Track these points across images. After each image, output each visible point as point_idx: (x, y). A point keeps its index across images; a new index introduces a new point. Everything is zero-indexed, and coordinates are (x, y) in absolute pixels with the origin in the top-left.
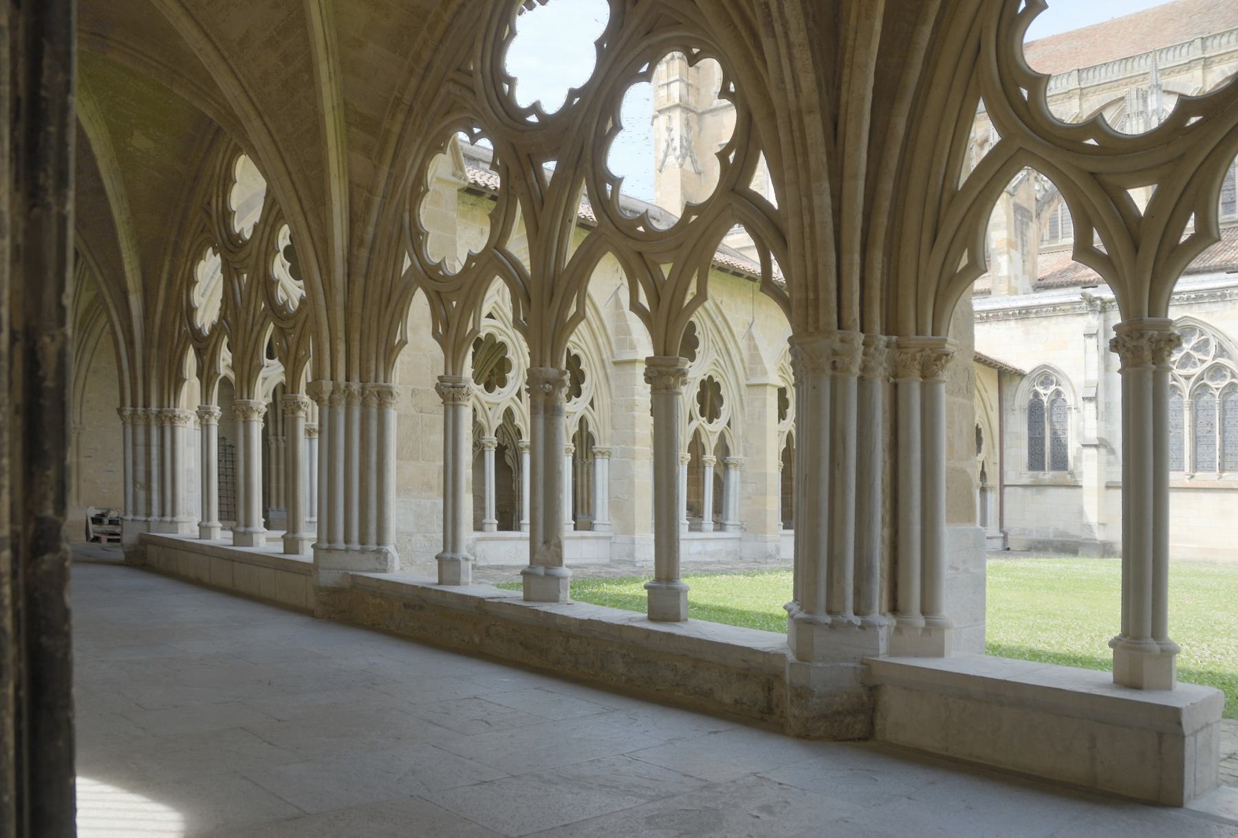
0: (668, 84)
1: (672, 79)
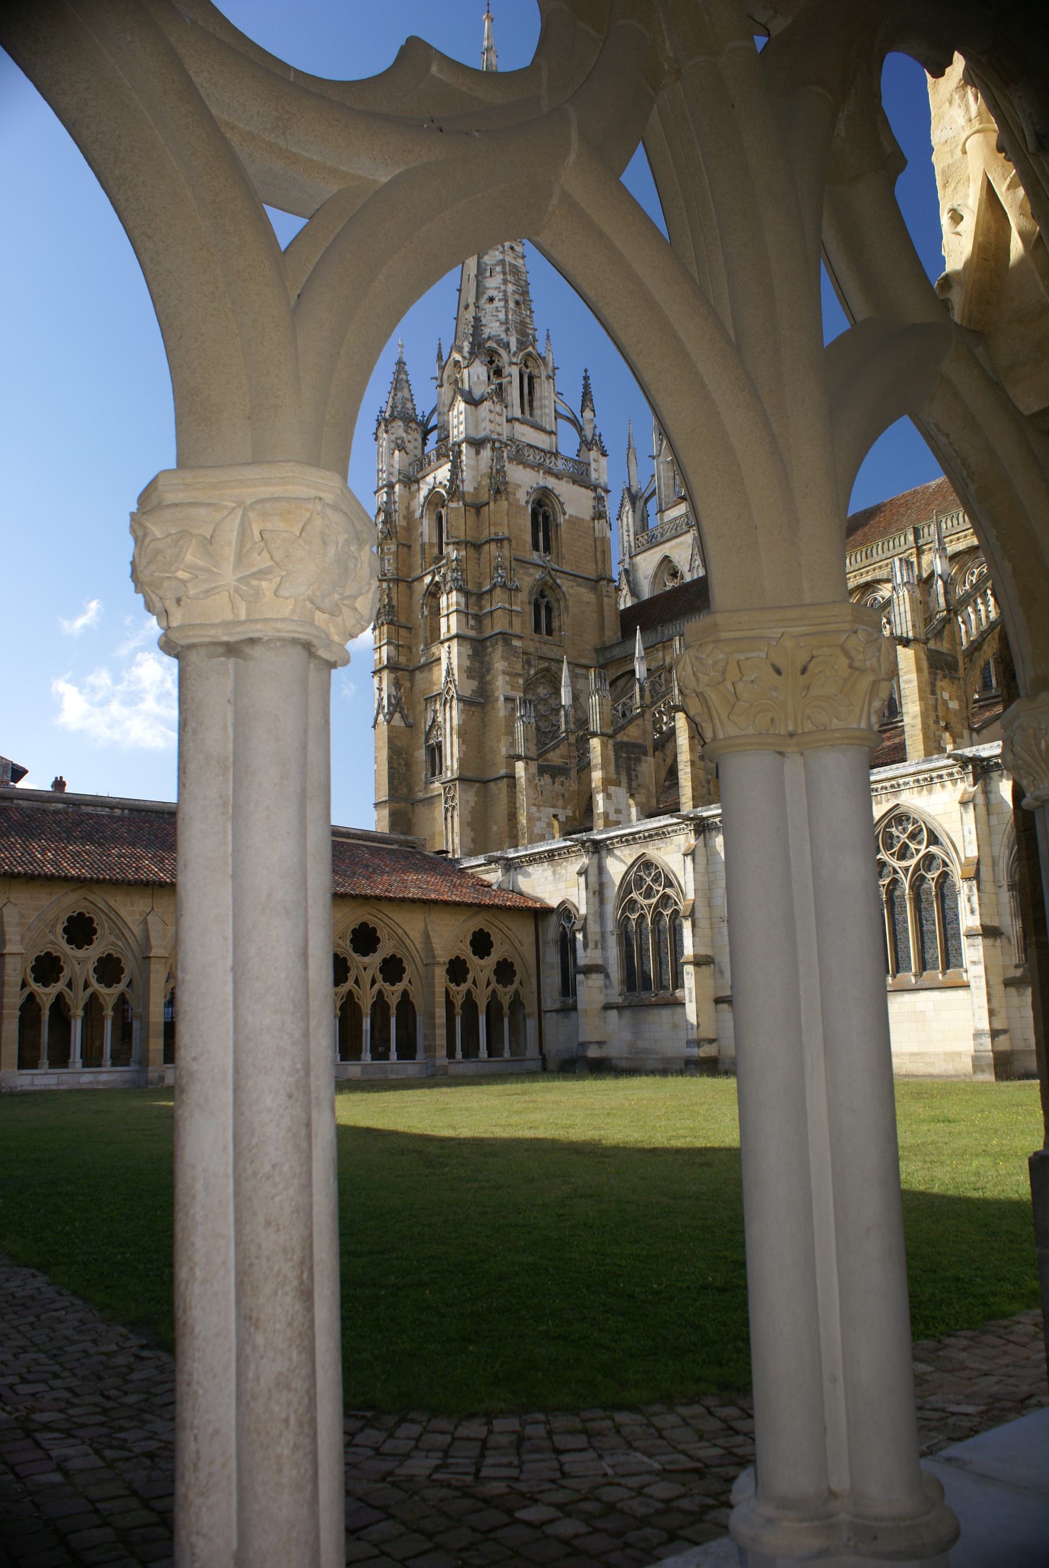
0: (380, 647)
1: (382, 643)
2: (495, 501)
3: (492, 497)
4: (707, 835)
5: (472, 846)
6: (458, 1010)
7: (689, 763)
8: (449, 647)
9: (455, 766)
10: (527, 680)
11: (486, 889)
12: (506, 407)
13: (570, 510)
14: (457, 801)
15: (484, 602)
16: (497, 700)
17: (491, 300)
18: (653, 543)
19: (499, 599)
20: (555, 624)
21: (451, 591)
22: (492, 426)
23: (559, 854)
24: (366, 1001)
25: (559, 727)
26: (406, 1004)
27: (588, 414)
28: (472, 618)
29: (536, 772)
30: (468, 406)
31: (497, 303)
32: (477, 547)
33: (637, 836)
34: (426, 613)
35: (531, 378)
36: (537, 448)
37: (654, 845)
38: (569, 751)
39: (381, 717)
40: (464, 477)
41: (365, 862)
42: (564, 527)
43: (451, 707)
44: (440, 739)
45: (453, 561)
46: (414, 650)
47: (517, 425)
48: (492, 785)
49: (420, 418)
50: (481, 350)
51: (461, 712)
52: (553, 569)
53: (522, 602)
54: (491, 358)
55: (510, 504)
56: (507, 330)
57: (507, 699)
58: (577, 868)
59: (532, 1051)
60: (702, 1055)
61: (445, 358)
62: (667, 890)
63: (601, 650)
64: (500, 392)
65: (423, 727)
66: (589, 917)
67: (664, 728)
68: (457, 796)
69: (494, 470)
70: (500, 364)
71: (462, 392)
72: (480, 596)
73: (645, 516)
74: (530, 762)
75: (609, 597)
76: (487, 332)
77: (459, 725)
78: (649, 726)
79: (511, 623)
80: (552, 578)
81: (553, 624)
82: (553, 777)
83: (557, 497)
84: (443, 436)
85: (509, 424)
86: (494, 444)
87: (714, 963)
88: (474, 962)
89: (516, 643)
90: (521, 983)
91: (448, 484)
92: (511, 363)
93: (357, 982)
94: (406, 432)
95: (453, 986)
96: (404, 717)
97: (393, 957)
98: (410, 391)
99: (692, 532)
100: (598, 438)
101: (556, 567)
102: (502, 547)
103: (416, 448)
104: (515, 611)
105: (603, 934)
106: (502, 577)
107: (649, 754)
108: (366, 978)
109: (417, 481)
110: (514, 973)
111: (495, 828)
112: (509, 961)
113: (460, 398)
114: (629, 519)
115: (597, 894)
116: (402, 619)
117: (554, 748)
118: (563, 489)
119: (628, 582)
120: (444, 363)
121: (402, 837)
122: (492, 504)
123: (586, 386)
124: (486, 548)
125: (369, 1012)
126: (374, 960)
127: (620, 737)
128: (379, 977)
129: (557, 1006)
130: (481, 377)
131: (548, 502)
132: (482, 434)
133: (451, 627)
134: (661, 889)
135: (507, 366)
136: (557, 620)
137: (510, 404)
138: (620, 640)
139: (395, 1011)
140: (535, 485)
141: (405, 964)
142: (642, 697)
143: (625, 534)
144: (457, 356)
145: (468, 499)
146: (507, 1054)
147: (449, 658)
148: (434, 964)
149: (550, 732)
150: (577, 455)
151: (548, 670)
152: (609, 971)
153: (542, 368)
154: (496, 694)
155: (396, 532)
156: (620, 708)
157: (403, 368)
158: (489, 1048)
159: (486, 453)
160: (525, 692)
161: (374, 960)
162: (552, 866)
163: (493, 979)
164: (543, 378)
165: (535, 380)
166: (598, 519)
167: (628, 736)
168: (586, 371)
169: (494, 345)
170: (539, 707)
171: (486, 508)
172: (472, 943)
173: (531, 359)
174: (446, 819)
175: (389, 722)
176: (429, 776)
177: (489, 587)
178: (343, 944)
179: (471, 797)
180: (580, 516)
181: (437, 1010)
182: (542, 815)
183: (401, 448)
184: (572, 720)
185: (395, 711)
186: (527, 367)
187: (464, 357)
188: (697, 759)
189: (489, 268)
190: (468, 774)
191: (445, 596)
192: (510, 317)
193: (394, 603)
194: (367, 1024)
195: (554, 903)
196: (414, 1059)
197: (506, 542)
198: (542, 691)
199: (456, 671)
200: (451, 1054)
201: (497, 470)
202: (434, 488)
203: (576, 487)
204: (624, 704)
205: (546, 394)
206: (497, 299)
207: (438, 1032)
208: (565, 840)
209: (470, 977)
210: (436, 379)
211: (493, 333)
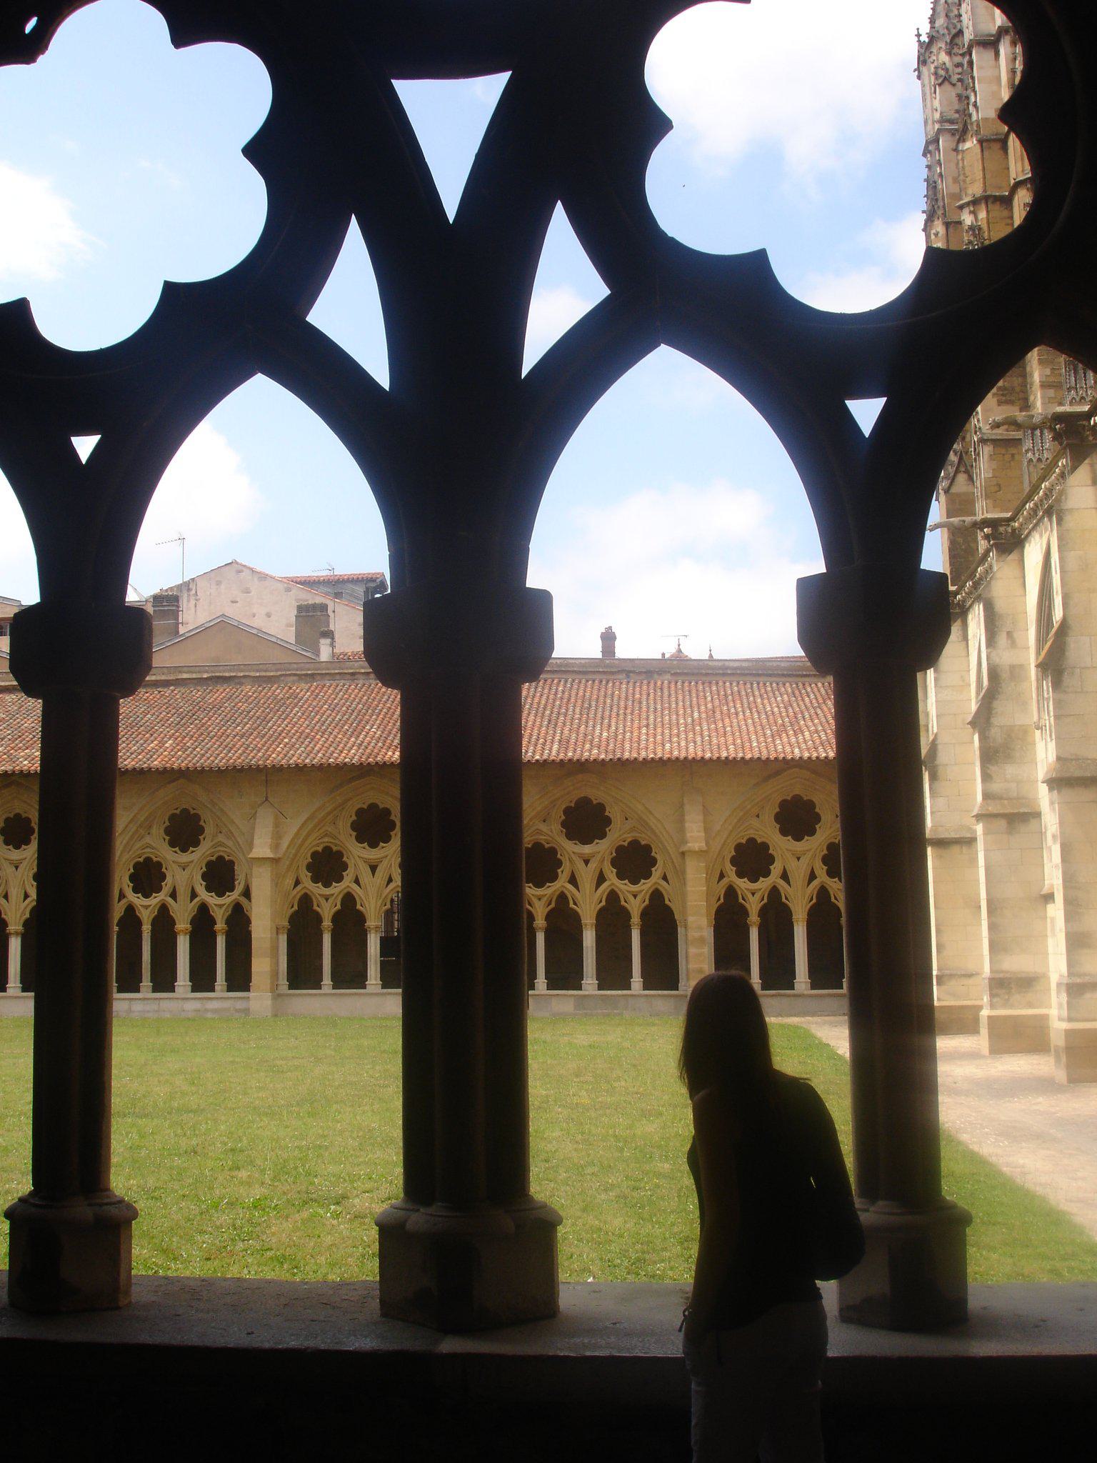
88: (781, 846)
93: (573, 880)
108: (587, 876)
126: (602, 849)
128: (611, 873)
194: (589, 939)
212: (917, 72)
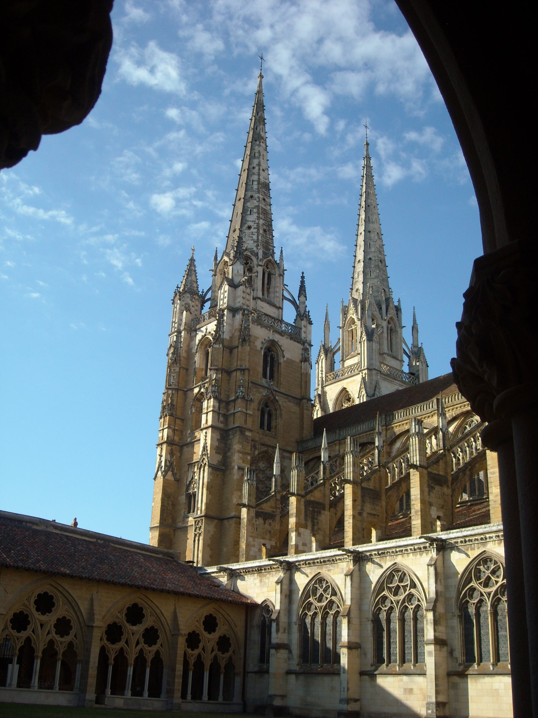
1: (165, 427)
2: (242, 346)
3: (240, 343)
4: (361, 563)
5: (209, 559)
6: (191, 667)
7: (352, 517)
8: (206, 433)
9: (203, 508)
10: (252, 458)
11: (216, 588)
12: (253, 290)
13: (287, 355)
14: (202, 530)
15: (230, 407)
16: (233, 468)
17: (249, 228)
18: (336, 378)
19: (239, 407)
20: (273, 424)
21: (210, 398)
22: (244, 301)
23: (265, 569)
24: (132, 657)
25: (271, 489)
26: (157, 659)
27: (302, 298)
28: (222, 416)
29: (254, 515)
30: (230, 288)
31: (252, 230)
32: (229, 373)
33: (316, 561)
34: (194, 411)
35: (270, 275)
36: (269, 316)
37: (326, 568)
38: (276, 503)
39: (160, 473)
40: (224, 330)
41: (140, 564)
42: (283, 365)
43: (204, 470)
44: (196, 490)
45: (213, 380)
46: (184, 433)
47: (259, 302)
48: (226, 522)
49: (200, 293)
50: (241, 256)
51: (210, 474)
52: (274, 390)
53: (254, 409)
54: (247, 261)
55: (251, 349)
56: (258, 246)
57: (239, 468)
58: (276, 579)
59: (237, 698)
60: (350, 709)
61: (219, 259)
62: (333, 598)
63: (301, 442)
64: (250, 282)
65: (185, 481)
66: (281, 612)
67: (337, 494)
68: (203, 527)
69: (243, 327)
70: (252, 265)
71: (227, 279)
72: (228, 403)
73: (333, 362)
74: (251, 509)
75: (307, 410)
76: (245, 246)
77: (208, 482)
78: (328, 492)
79: (246, 421)
80: (273, 395)
81: (272, 424)
82: (265, 520)
83: (280, 346)
84: (213, 305)
85: (254, 301)
86: (244, 311)
87: (360, 648)
89: (248, 434)
90: (234, 652)
91: (214, 333)
92: (258, 265)
93: (127, 642)
94: (191, 300)
95: (189, 651)
96: (174, 474)
97: (152, 628)
98: (196, 276)
99: (361, 374)
100: (307, 313)
101: (276, 389)
102: (244, 374)
103: (197, 311)
104: (250, 414)
105: (289, 624)
106: (242, 392)
107: (326, 509)
109: (196, 330)
110: (230, 645)
111: (225, 550)
112: (227, 636)
113: (226, 283)
114: (323, 363)
115: (288, 596)
116: (179, 413)
117: (268, 500)
118: (284, 342)
119: (320, 402)
120: (218, 262)
121: (166, 550)
122: (240, 347)
123: (303, 282)
124: (234, 374)
125: (133, 663)
126: (139, 629)
127: (309, 497)
128: (142, 640)
129: (256, 669)
130: (239, 272)
131: (274, 349)
132: (238, 305)
133: (209, 421)
134: (329, 596)
135: (255, 267)
136: (274, 422)
137: (255, 289)
138: (313, 437)
139: (150, 664)
140: (267, 338)
141: (159, 633)
142: (324, 473)
143: (320, 372)
144: (226, 259)
145: (226, 343)
146: (221, 699)
147: (206, 440)
148: (178, 635)
149: (264, 491)
150: (294, 323)
151: (266, 452)
152: (292, 648)
153: (277, 269)
154: (233, 464)
155: (180, 360)
156: (310, 479)
157: (194, 263)
158: (209, 694)
159: (239, 317)
160: (251, 464)
161: (139, 629)
162: (260, 577)
163: (216, 648)
164: (277, 275)
165: (272, 276)
166: (304, 362)
167: (314, 497)
168: (303, 273)
169: (249, 254)
170: (259, 475)
171: (236, 350)
172: (204, 623)
173: (270, 264)
174: (194, 541)
175: (164, 477)
176: (186, 513)
177: (234, 398)
178: (120, 616)
179: (212, 528)
180: (293, 359)
181: (177, 666)
182: (256, 543)
183: (188, 310)
184: (279, 484)
185: (169, 470)
186: (268, 268)
187: (230, 259)
188: (357, 515)
189: (250, 209)
190: (211, 514)
191: (206, 401)
192: (260, 238)
193: (175, 403)
194: (130, 671)
195: (259, 601)
196: (159, 697)
197: (246, 371)
198: (262, 465)
199: (209, 448)
200: (184, 696)
201: (245, 327)
202: (205, 335)
203: (292, 342)
204: (313, 477)
205: (278, 285)
206: (253, 227)
207: (176, 680)
208: (269, 560)
209: (201, 645)
210: (212, 270)
211: (249, 247)
212: (172, 301)
